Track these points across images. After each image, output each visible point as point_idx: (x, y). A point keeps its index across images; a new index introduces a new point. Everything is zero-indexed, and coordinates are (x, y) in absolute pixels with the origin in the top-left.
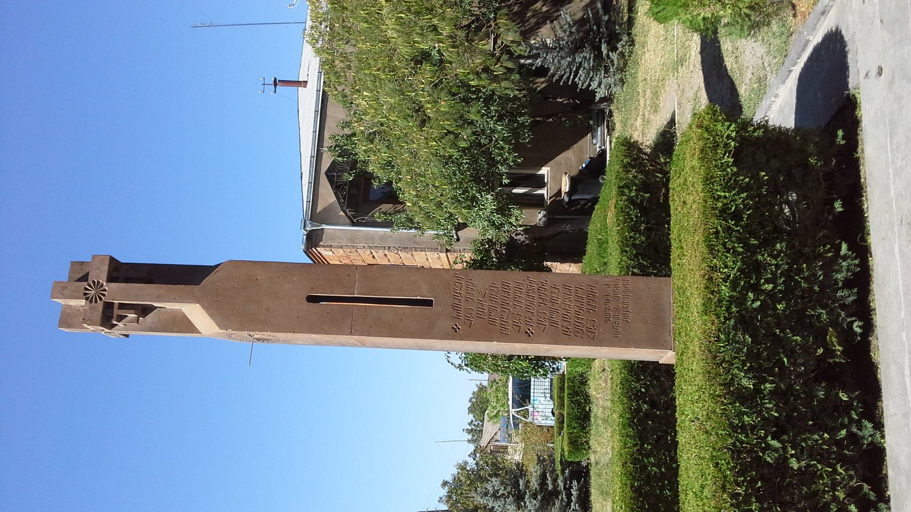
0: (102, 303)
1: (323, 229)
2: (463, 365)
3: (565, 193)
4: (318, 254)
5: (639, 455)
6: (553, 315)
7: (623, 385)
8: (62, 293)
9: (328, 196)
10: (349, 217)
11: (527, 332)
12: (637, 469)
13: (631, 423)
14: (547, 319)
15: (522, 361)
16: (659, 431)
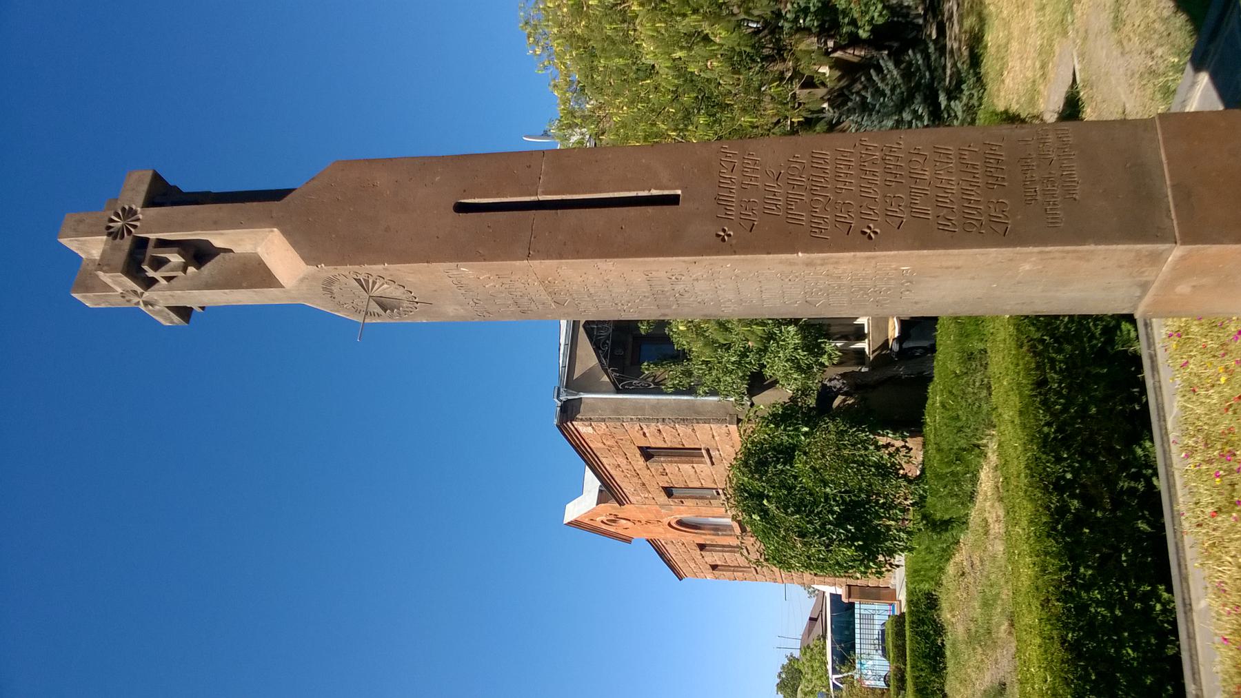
2: (762, 560)
3: (893, 340)
4: (575, 432)
5: (1070, 586)
7: (1031, 469)
8: (75, 229)
9: (588, 358)
10: (614, 383)
11: (865, 233)
12: (1069, 610)
13: (1051, 531)
14: (906, 207)
15: (845, 547)
16: (1104, 546)
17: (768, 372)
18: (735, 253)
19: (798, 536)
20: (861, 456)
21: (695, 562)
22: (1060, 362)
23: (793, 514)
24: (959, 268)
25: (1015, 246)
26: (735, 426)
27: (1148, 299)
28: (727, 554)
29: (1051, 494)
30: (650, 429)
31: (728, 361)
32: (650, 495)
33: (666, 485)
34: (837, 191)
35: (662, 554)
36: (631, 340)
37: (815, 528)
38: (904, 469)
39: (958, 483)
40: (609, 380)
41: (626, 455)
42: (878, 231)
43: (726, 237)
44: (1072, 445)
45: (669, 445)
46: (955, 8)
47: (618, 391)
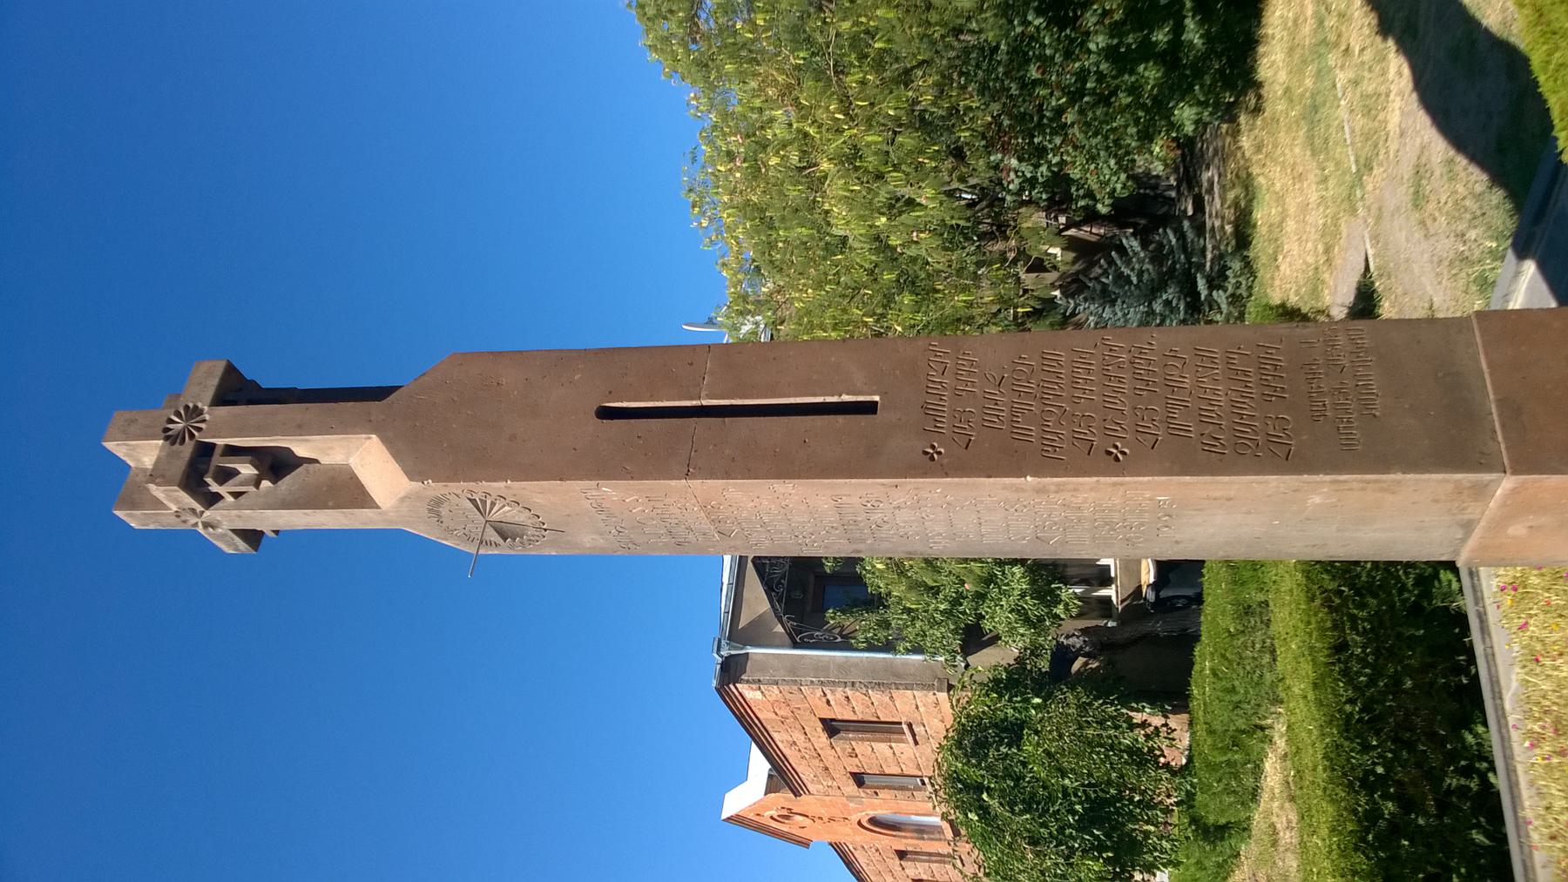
0: (193, 442)
1: (748, 653)
2: (981, 875)
3: (1148, 586)
4: (740, 698)
6: (1175, 413)
7: (1330, 760)
9: (758, 601)
10: (790, 635)
13: (1359, 843)
14: (1160, 421)
15: (1091, 859)
16: (1429, 863)
17: (987, 625)
18: (947, 475)
19: (1029, 844)
20: (1109, 737)
21: (893, 875)
22: (1364, 620)
23: (1022, 813)
24: (1230, 499)
25: (1300, 473)
26: (946, 694)
27: (1471, 543)
28: (935, 864)
29: (1358, 793)
30: (835, 696)
31: (936, 610)
32: (835, 783)
33: (856, 770)
34: (1075, 401)
35: (849, 864)
36: (812, 579)
37: (1050, 833)
38: (1165, 757)
39: (1236, 776)
40: (783, 631)
41: (804, 728)
42: (1126, 450)
43: (935, 456)
44: (1381, 730)
45: (860, 717)
46: (1216, 179)
47: (795, 645)
